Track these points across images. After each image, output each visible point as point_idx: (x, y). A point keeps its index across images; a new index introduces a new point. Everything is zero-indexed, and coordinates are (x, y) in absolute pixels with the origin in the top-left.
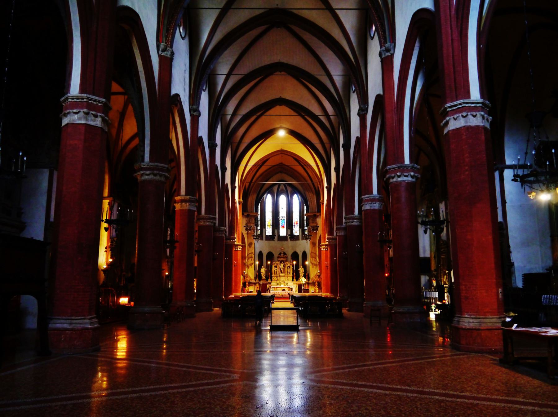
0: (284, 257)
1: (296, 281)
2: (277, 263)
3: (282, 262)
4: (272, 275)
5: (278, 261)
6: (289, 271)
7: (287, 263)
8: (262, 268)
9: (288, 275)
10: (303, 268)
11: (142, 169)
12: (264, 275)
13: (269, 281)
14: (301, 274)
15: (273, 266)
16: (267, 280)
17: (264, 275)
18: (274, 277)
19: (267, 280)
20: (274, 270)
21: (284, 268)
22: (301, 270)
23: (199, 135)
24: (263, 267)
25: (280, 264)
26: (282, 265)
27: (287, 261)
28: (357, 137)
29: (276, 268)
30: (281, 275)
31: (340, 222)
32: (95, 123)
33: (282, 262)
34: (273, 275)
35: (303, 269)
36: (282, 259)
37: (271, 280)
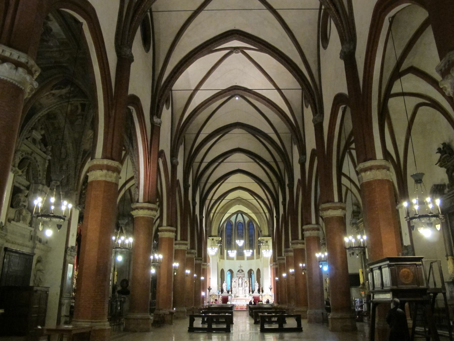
1: (252, 293)
2: (236, 278)
3: (241, 278)
5: (237, 277)
6: (246, 286)
7: (245, 278)
8: (224, 283)
10: (258, 282)
11: (137, 208)
13: (230, 293)
14: (256, 288)
15: (233, 281)
16: (228, 292)
19: (228, 292)
21: (242, 283)
23: (177, 178)
26: (240, 280)
27: (244, 277)
28: (299, 180)
30: (239, 288)
31: (287, 246)
32: (111, 179)
35: (258, 283)
36: (240, 275)
37: (232, 293)
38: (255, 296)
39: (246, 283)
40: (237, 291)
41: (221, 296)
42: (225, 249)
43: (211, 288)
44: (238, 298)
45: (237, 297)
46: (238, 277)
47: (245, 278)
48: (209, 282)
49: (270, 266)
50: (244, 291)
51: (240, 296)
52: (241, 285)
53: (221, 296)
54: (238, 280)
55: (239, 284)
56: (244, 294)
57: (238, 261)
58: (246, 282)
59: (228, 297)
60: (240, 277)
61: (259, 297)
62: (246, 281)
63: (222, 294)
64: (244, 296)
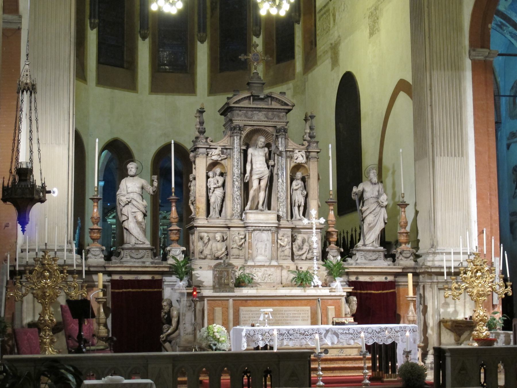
0: (275, 105)
4: (193, 219)
6: (299, 198)
7: (292, 145)
8: (124, 174)
9: (299, 224)
12: (138, 223)
14: (369, 219)
17: (140, 217)
18: (205, 235)
20: (208, 189)
21: (271, 179)
22: (366, 195)
24: (132, 168)
25: (245, 153)
29: (221, 180)
33: (262, 140)
34: (201, 220)
38: (362, 279)
39: (297, 184)
40: (236, 235)
41: (101, 279)
42: (92, 28)
43: (37, 179)
44: (246, 291)
45: (240, 283)
46: (240, 129)
47: (292, 145)
48: (31, 107)
49: (468, 63)
50: (286, 241)
51: (258, 275)
52: (262, 195)
53: (101, 279)
54: (236, 155)
55: (246, 187)
56: (288, 263)
57: (160, 99)
58: (299, 175)
59: (159, 284)
60: (256, 132)
61: (392, 285)
62: (298, 167)
63: (115, 265)
64: (288, 276)
